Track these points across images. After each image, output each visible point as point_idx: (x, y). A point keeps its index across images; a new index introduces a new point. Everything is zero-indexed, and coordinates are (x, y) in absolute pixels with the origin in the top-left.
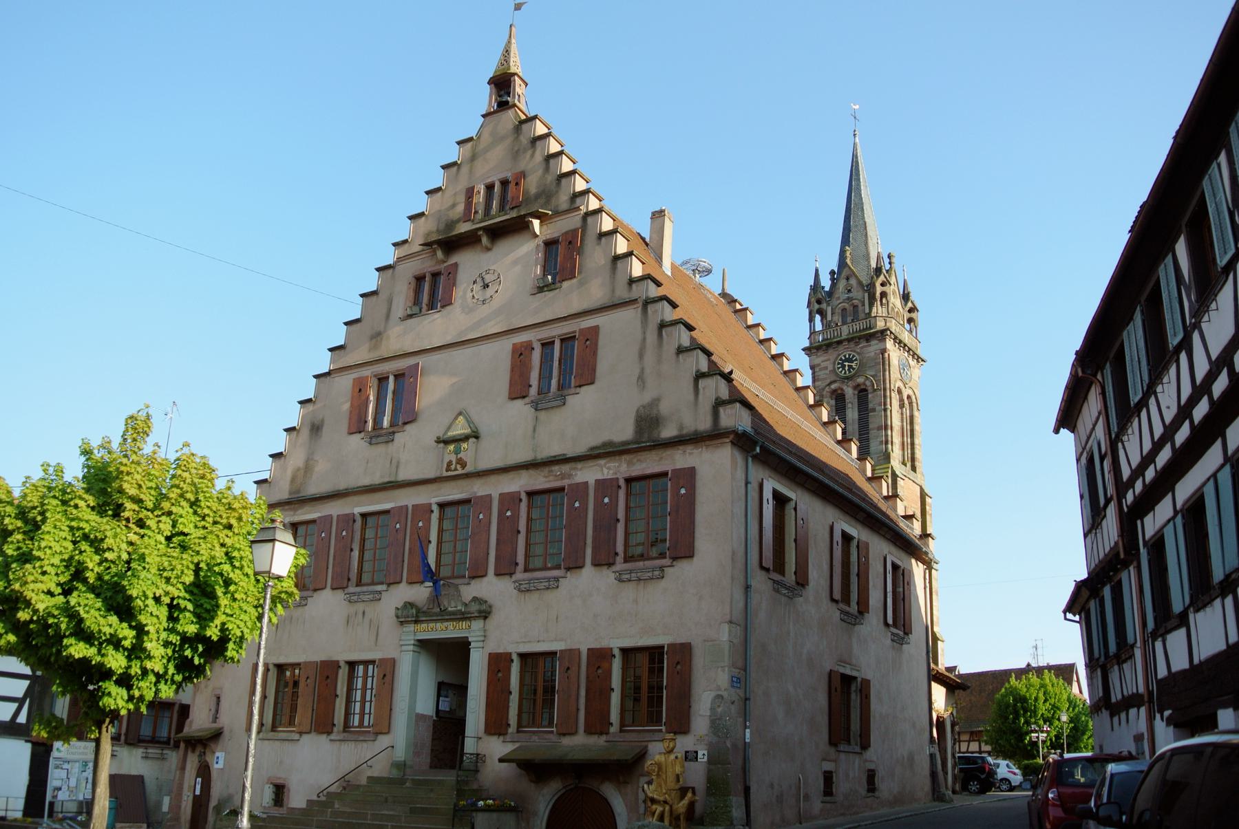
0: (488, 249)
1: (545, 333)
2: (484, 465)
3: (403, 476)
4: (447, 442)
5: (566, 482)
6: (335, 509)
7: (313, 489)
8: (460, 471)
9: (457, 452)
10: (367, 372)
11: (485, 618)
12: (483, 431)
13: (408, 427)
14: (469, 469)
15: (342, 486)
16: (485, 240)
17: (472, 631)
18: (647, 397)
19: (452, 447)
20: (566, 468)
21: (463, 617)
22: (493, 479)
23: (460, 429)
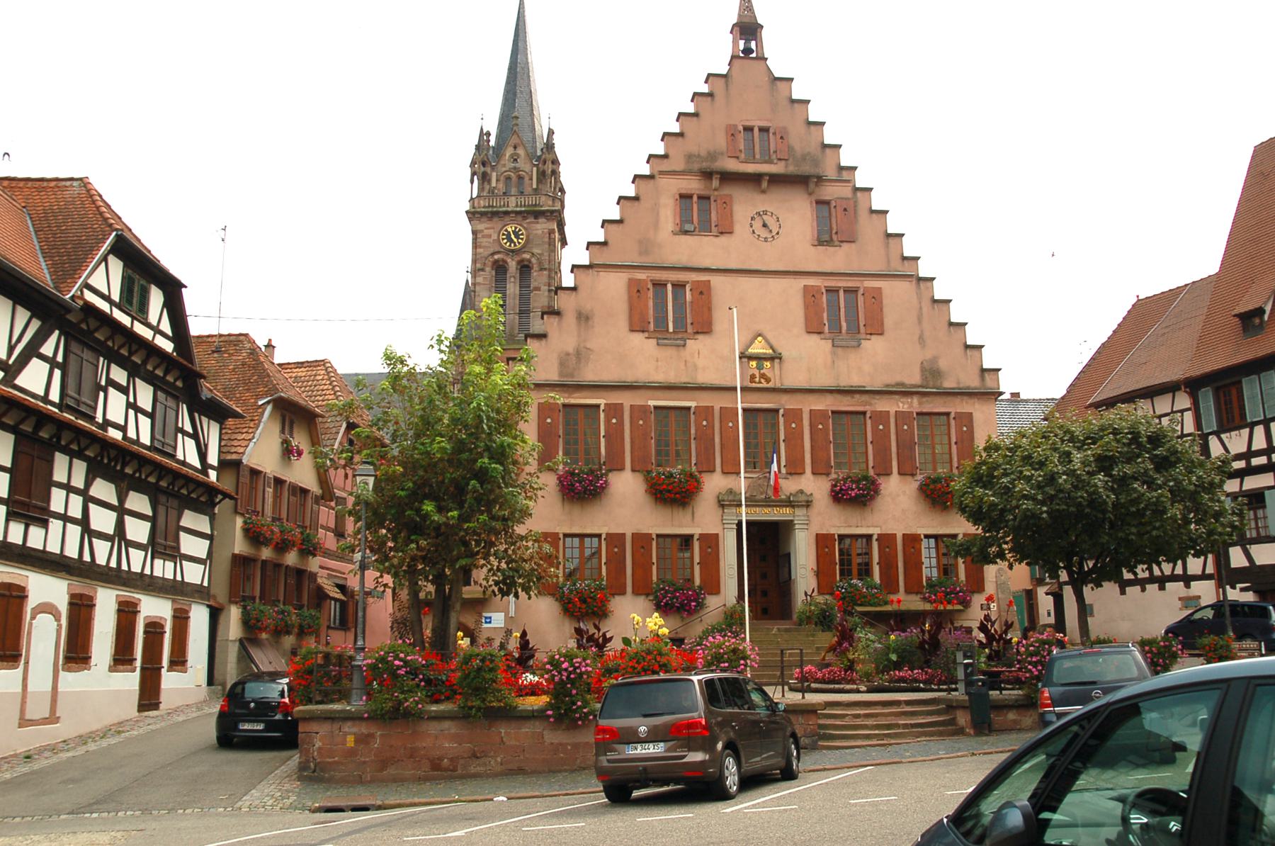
0: (763, 192)
1: (832, 283)
2: (789, 383)
3: (704, 378)
4: (751, 358)
5: (867, 408)
6: (627, 400)
7: (590, 374)
8: (764, 385)
9: (759, 367)
10: (642, 275)
11: (808, 506)
12: (785, 354)
13: (700, 337)
14: (771, 385)
15: (629, 377)
16: (765, 184)
17: (798, 516)
18: (928, 354)
19: (754, 363)
20: (865, 398)
21: (789, 503)
22: (799, 396)
23: (758, 348)
